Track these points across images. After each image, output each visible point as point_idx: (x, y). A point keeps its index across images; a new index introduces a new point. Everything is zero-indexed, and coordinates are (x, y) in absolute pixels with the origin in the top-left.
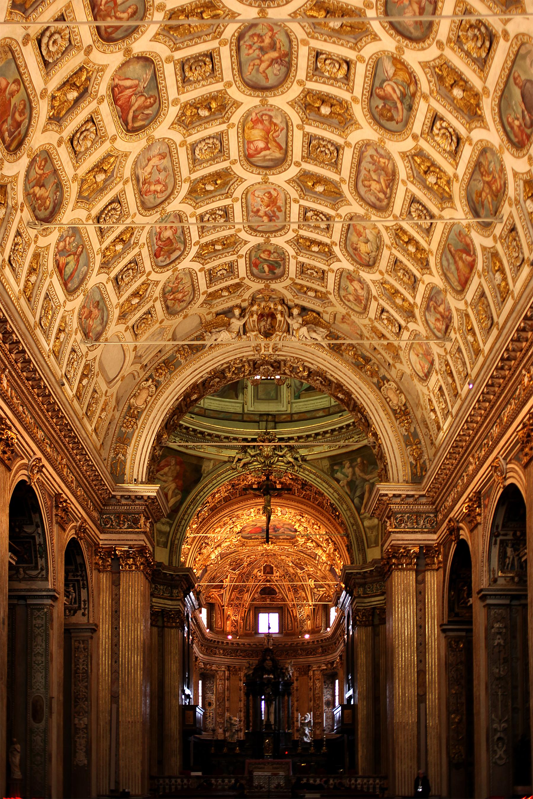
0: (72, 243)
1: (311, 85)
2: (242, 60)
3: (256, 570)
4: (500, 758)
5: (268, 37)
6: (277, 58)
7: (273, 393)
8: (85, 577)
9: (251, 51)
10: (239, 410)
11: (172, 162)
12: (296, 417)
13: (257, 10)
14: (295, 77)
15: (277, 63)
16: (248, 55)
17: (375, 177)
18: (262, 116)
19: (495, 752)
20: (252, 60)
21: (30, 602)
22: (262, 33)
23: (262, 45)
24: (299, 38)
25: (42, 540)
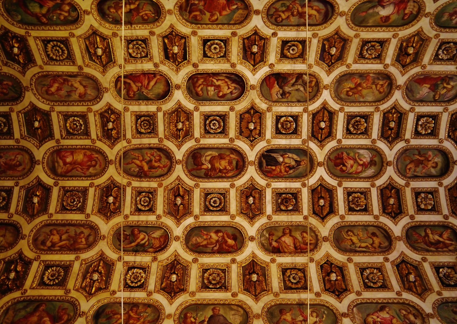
1: (129, 190)
2: (143, 150)
5: (159, 164)
6: (144, 170)
9: (149, 155)
11: (75, 101)
13: (181, 159)
14: (133, 180)
15: (140, 170)
16: (147, 154)
17: (64, 237)
18: (95, 161)
20: (142, 156)
22: (161, 161)
23: (153, 161)
24: (163, 182)
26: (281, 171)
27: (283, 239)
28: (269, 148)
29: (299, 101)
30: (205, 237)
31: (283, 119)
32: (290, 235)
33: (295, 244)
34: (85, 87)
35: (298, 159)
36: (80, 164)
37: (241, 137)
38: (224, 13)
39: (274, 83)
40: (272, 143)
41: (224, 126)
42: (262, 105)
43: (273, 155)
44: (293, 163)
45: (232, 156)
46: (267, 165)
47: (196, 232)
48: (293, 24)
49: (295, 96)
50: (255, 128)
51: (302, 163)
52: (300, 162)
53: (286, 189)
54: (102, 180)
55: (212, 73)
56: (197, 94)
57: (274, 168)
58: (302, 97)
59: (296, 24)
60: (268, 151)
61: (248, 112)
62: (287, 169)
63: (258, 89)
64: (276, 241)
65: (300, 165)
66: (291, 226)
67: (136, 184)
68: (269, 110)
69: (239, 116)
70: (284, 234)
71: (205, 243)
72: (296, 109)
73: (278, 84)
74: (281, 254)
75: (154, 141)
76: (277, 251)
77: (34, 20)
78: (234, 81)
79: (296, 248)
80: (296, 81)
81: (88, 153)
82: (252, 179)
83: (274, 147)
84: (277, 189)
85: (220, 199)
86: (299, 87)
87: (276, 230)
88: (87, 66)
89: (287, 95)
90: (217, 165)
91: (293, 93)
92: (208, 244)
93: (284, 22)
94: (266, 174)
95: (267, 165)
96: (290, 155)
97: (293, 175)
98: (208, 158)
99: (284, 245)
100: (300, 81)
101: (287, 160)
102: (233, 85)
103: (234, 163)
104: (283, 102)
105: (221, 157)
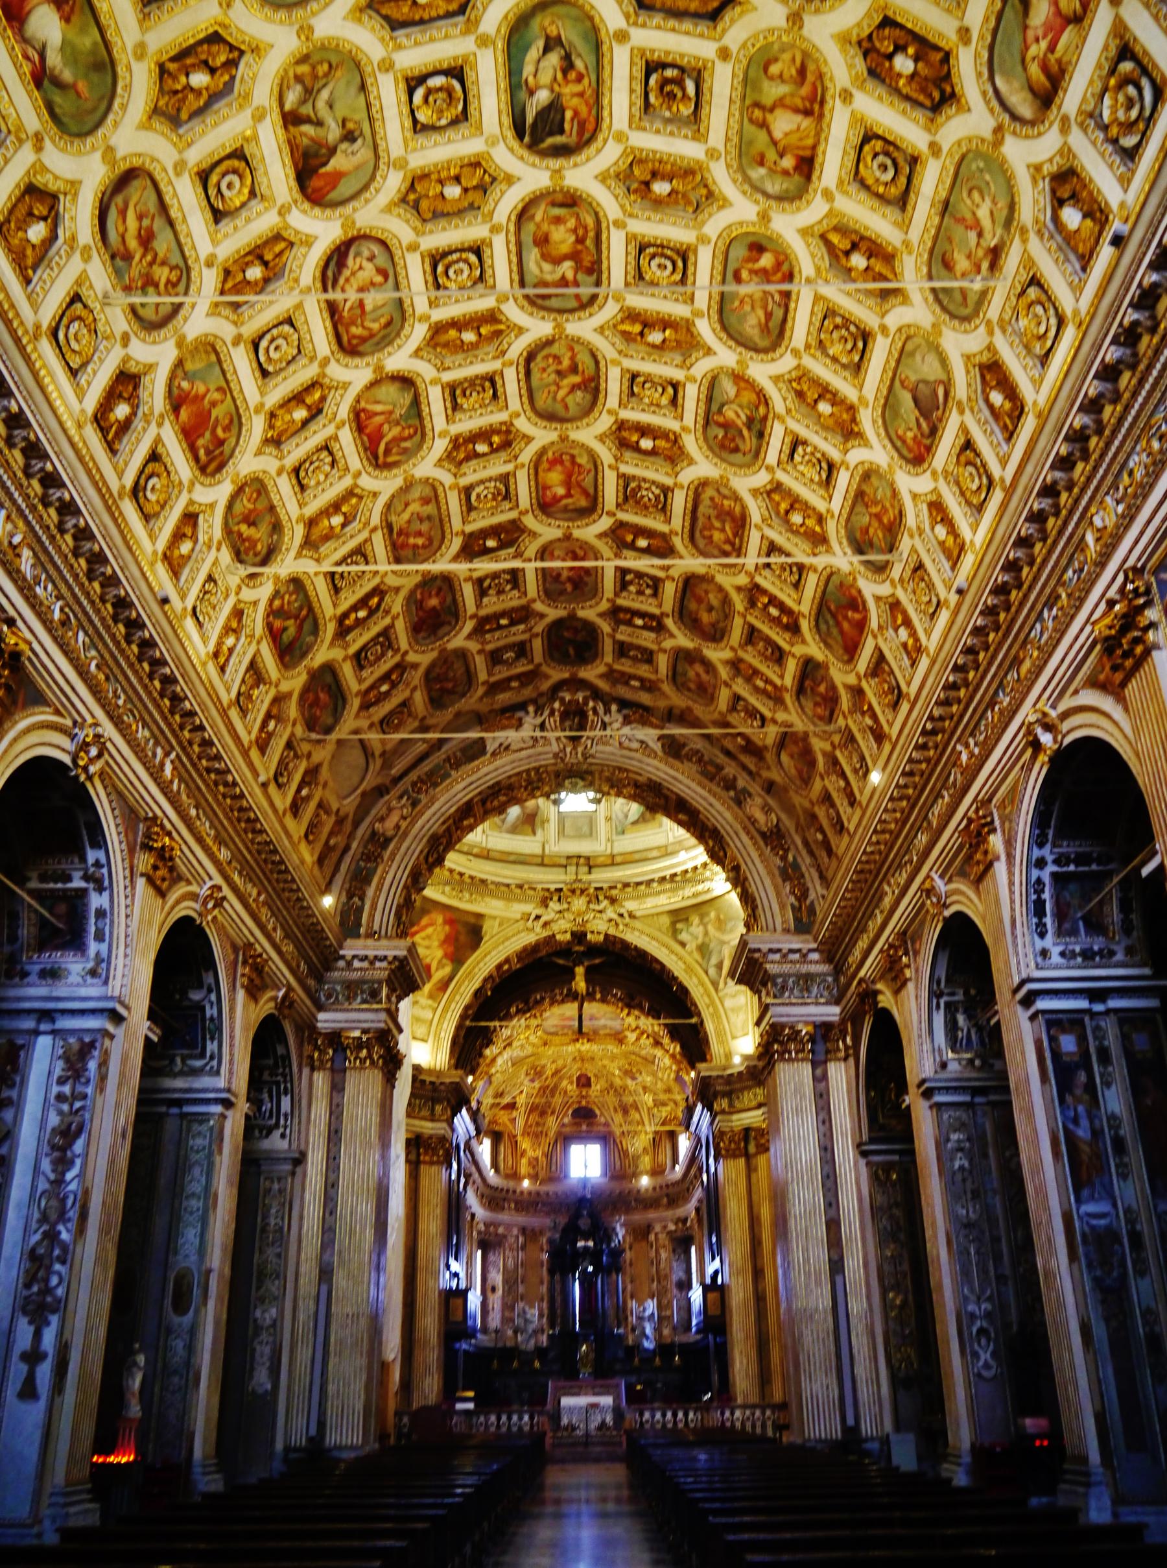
0: (291, 601)
3: (564, 1083)
4: (987, 1366)
7: (586, 829)
8: (288, 1077)
10: (538, 851)
12: (618, 859)
19: (975, 1355)
21: (188, 1109)
25: (215, 1012)
26: (581, 95)
27: (778, 134)
28: (510, 134)
29: (363, 87)
30: (747, 308)
31: (423, 116)
32: (772, 110)
33: (796, 111)
34: (407, 505)
35: (541, 44)
36: (569, 476)
37: (486, 209)
38: (201, 389)
39: (327, 174)
40: (497, 131)
41: (462, 250)
42: (392, 183)
43: (530, 119)
44: (554, 59)
45: (538, 218)
46: (561, 131)
47: (732, 320)
48: (171, 236)
49: (350, 105)
50: (457, 179)
51: (553, 31)
52: (548, 38)
53: (632, 91)
54: (606, 455)
55: (332, 316)
56: (389, 324)
57: (569, 114)
58: (348, 83)
59: (169, 230)
60: (520, 134)
61: (416, 206)
62: (572, 75)
63: (348, 209)
64: (781, 156)
65: (559, 37)
66: (743, 98)
67: (612, 401)
68: (401, 164)
69: (429, 226)
70: (764, 125)
71: (761, 313)
72: (388, 93)
73: (325, 164)
74: (818, 160)
75: (510, 375)
76: (807, 165)
77: (307, 626)
78: (341, 265)
79: (807, 113)
80: (308, 120)
81: (545, 465)
82: (603, 178)
83: (507, 121)
84: (631, 116)
85: (653, 257)
86: (321, 104)
87: (750, 143)
88: (368, 523)
89: (350, 126)
90: (565, 248)
91: (341, 111)
92: (765, 307)
93: (176, 259)
94: (587, 135)
95: (561, 131)
96: (528, 70)
97: (591, 60)
98: (547, 267)
99: (793, 140)
100: (306, 110)
101: (545, 78)
102: (350, 261)
103: (557, 211)
104: (374, 134)
105: (542, 241)
